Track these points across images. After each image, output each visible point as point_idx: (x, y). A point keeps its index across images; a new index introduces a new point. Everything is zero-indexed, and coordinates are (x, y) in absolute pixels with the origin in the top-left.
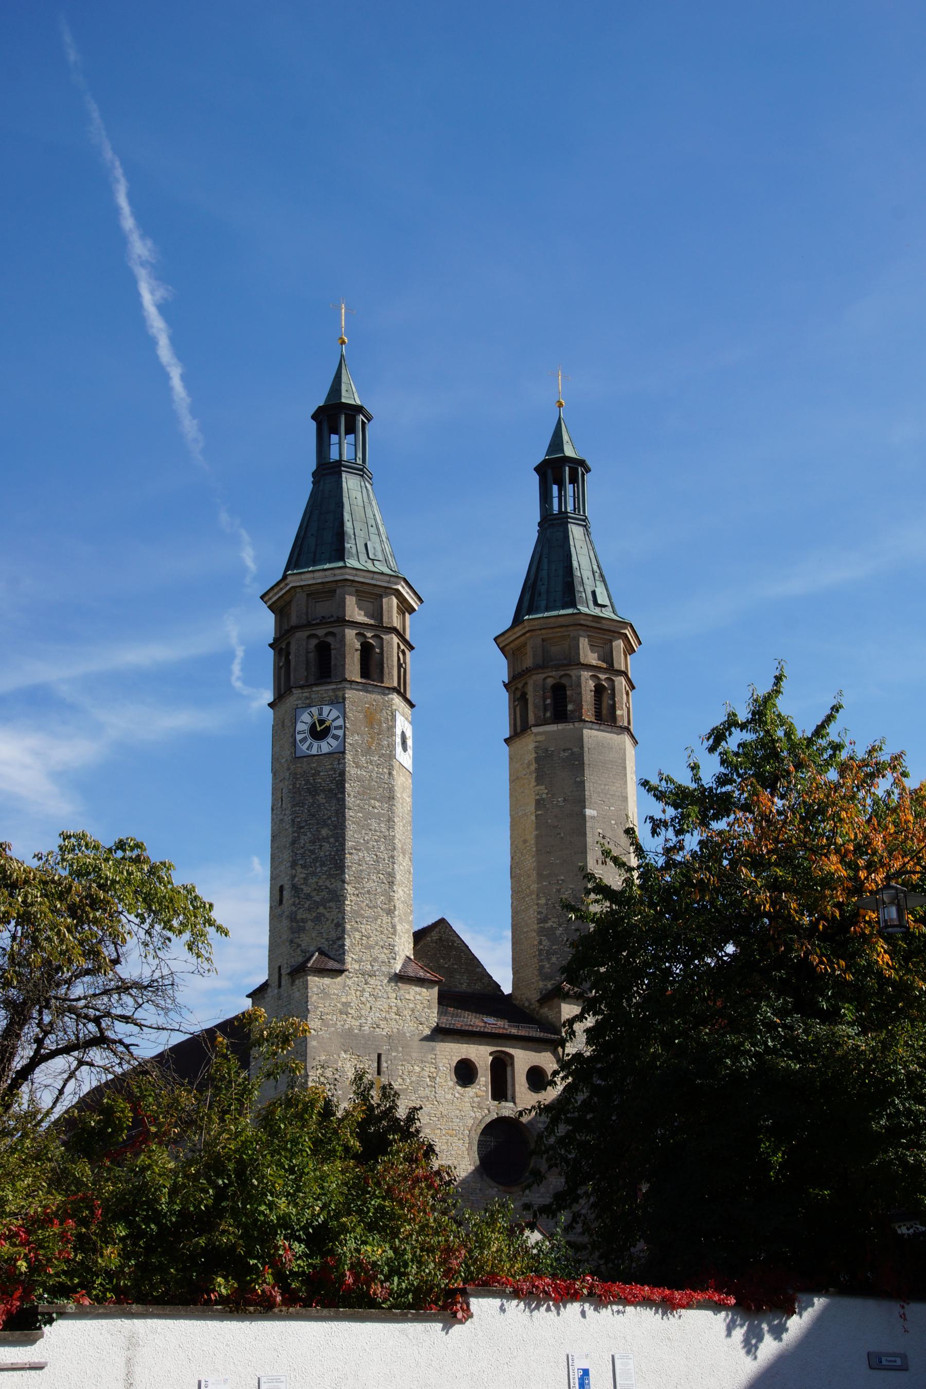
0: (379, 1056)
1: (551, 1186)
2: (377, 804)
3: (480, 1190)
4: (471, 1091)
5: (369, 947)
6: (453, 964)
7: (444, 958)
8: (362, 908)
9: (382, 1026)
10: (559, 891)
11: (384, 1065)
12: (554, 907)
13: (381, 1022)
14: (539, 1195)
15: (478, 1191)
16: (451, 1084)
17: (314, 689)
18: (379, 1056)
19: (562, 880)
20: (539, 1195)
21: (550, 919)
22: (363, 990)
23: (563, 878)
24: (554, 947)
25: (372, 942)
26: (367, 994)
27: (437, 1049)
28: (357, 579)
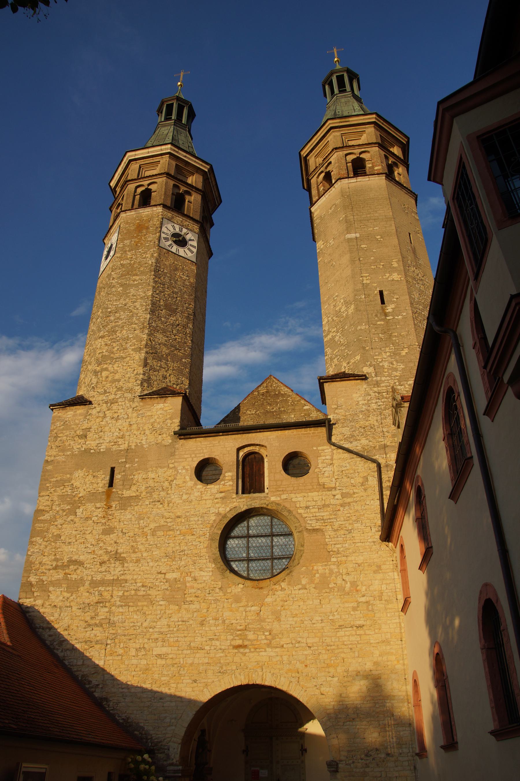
0: (113, 470)
1: (317, 575)
2: (137, 278)
3: (220, 589)
4: (213, 488)
5: (114, 381)
6: (279, 408)
7: (270, 405)
8: (113, 353)
9: (120, 443)
10: (335, 306)
11: (117, 477)
12: (333, 320)
13: (119, 440)
14: (300, 586)
15: (217, 590)
16: (190, 484)
17: (111, 232)
18: (113, 470)
19: (337, 296)
20: (300, 586)
21: (331, 332)
22: (105, 416)
23: (337, 294)
24: (335, 352)
25: (117, 377)
26: (108, 419)
27: (177, 453)
28: (136, 157)
